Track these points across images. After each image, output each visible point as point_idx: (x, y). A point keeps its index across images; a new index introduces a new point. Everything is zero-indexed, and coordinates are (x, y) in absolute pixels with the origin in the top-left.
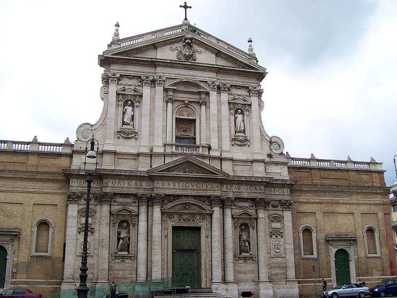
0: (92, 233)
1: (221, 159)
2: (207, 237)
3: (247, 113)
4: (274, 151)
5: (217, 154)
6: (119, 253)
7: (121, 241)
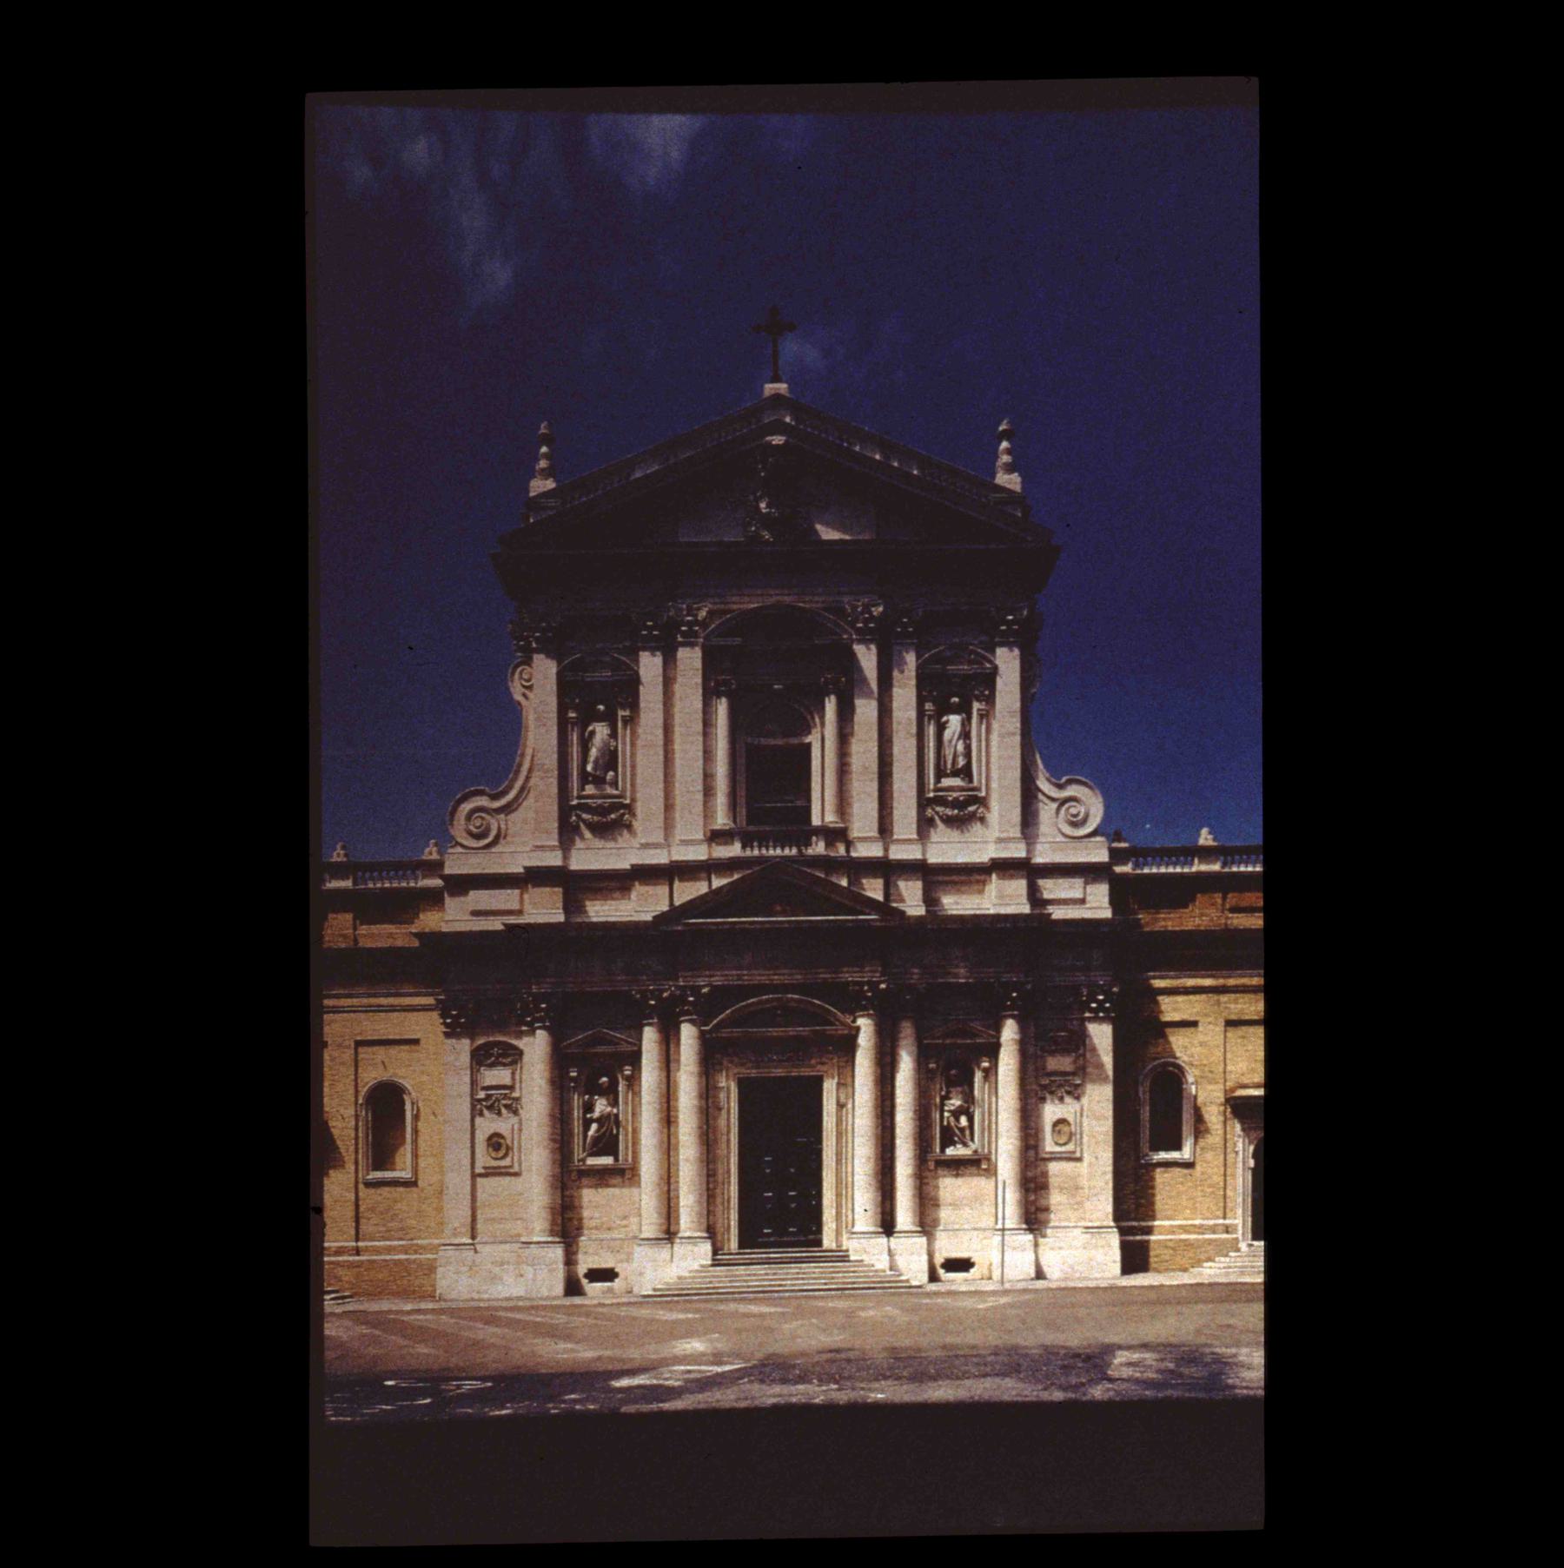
0: (516, 1112)
1: (888, 870)
2: (841, 1106)
3: (982, 706)
4: (1068, 830)
5: (873, 851)
6: (591, 1161)
7: (594, 1126)
